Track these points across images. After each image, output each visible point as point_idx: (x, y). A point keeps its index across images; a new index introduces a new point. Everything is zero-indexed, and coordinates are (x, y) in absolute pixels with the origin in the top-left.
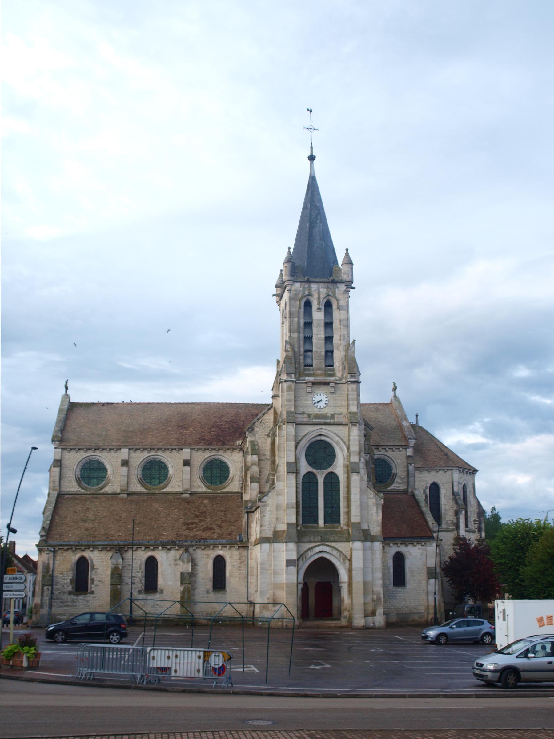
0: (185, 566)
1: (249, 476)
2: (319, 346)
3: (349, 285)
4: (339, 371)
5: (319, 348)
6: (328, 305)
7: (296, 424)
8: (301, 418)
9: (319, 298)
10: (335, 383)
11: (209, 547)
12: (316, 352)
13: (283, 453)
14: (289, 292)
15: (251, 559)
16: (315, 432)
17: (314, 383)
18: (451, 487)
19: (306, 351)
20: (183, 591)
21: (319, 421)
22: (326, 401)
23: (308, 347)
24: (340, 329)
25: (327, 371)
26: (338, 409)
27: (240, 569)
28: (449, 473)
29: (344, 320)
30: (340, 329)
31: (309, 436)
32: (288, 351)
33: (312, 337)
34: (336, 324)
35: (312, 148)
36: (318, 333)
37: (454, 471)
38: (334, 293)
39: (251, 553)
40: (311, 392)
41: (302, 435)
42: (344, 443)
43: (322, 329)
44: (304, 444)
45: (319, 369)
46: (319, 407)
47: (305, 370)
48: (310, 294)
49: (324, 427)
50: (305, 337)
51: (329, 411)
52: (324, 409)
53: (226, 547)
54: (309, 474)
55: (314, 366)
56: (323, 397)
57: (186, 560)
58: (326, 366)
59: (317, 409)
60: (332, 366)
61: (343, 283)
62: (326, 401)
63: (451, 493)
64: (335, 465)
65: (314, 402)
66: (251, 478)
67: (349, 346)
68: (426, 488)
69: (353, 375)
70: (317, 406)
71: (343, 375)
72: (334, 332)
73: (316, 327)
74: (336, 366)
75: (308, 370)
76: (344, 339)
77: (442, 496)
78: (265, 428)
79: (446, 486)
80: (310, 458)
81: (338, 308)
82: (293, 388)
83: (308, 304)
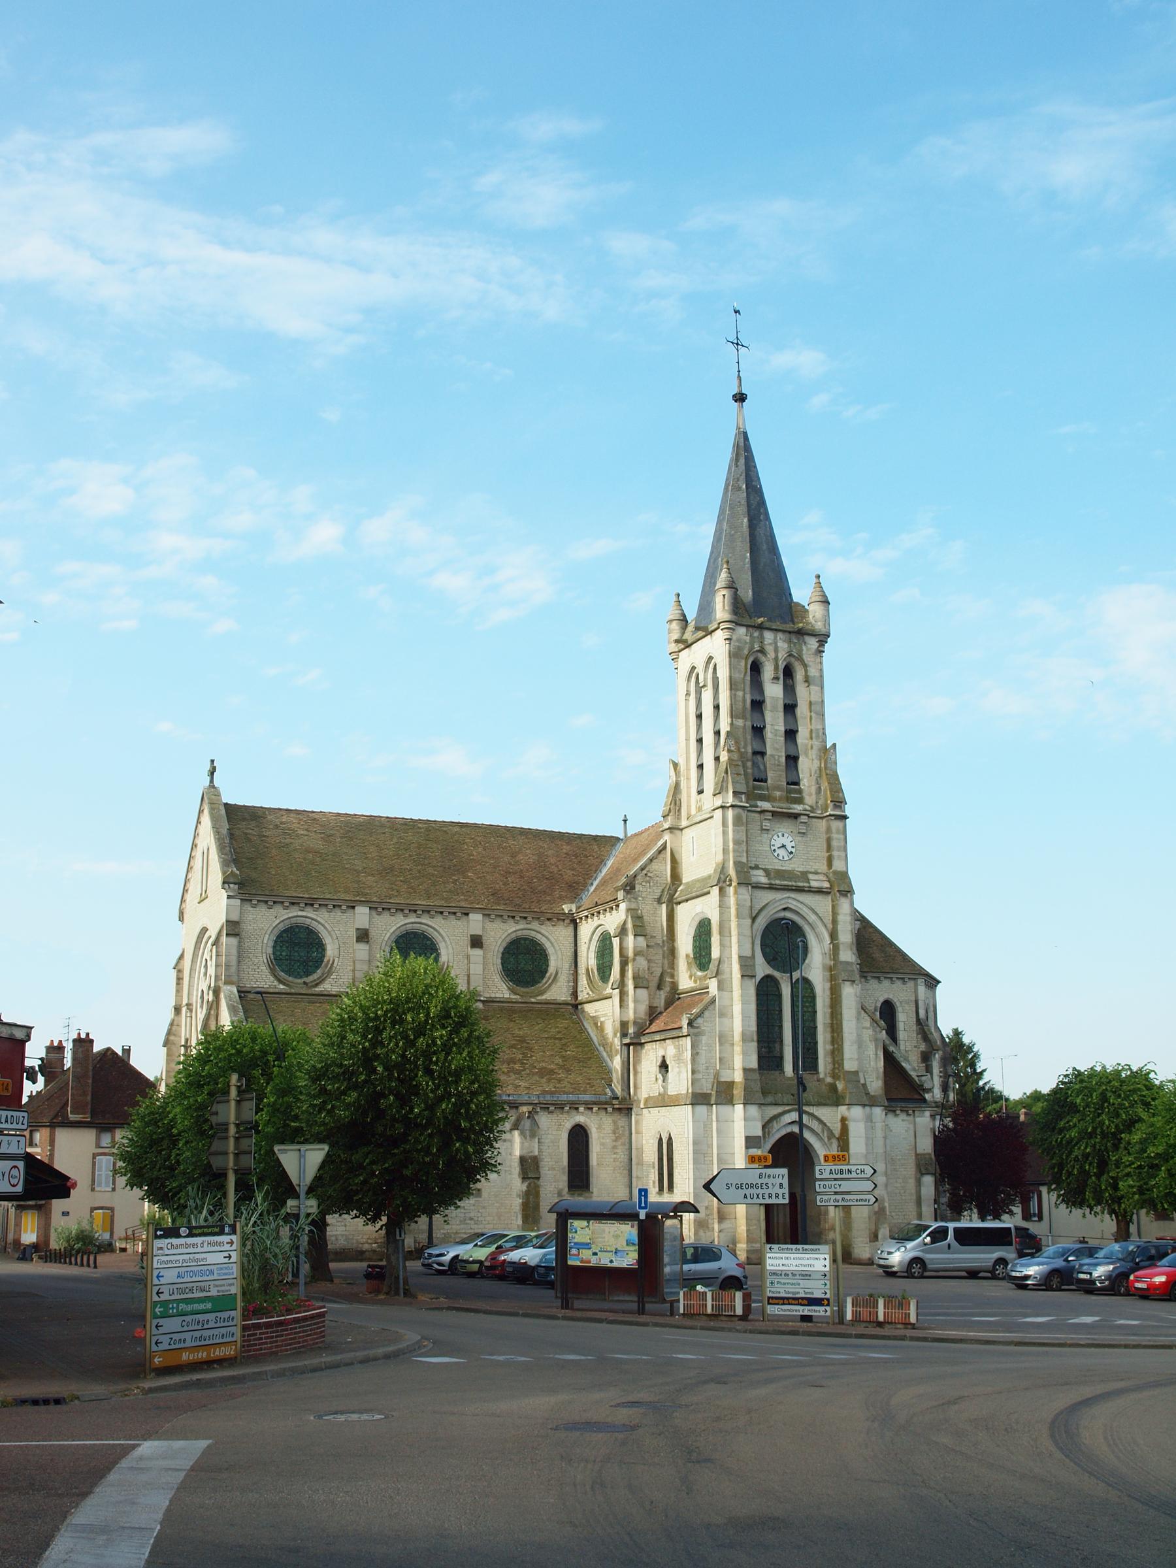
0: (526, 1144)
1: (630, 974)
2: (776, 746)
3: (823, 638)
4: (810, 795)
5: (777, 749)
6: (788, 672)
7: (753, 887)
8: (761, 878)
9: (776, 659)
10: (807, 815)
11: (563, 1108)
12: (772, 756)
13: (728, 938)
14: (727, 642)
15: (637, 1133)
16: (778, 903)
17: (774, 814)
18: (914, 1009)
19: (755, 753)
20: (526, 1191)
21: (783, 883)
22: (793, 847)
23: (758, 748)
24: (811, 716)
25: (790, 793)
26: (811, 864)
27: (616, 1151)
28: (911, 984)
29: (816, 703)
30: (811, 716)
31: (769, 909)
32: (732, 751)
33: (764, 727)
34: (802, 710)
35: (739, 377)
36: (775, 723)
37: (920, 981)
38: (800, 652)
39: (637, 1122)
40: (768, 830)
41: (758, 907)
42: (826, 926)
43: (781, 714)
44: (762, 922)
45: (778, 788)
46: (781, 858)
47: (755, 788)
48: (762, 651)
49: (792, 895)
50: (753, 726)
51: (797, 866)
52: (789, 862)
53: (592, 1108)
54: (768, 978)
55: (769, 781)
56: (787, 840)
57: (528, 1133)
58: (788, 784)
59: (777, 861)
60: (797, 784)
61: (814, 635)
62: (793, 847)
63: (915, 1020)
64: (809, 965)
65: (773, 848)
66: (635, 978)
67: (827, 753)
68: (876, 1010)
69: (837, 804)
70: (778, 855)
71: (817, 802)
72: (799, 723)
73: (771, 711)
74: (804, 785)
75: (760, 788)
76: (818, 737)
77: (901, 1026)
78: (653, 886)
79: (907, 1007)
80: (768, 950)
81: (806, 681)
82: (745, 820)
83: (756, 668)
